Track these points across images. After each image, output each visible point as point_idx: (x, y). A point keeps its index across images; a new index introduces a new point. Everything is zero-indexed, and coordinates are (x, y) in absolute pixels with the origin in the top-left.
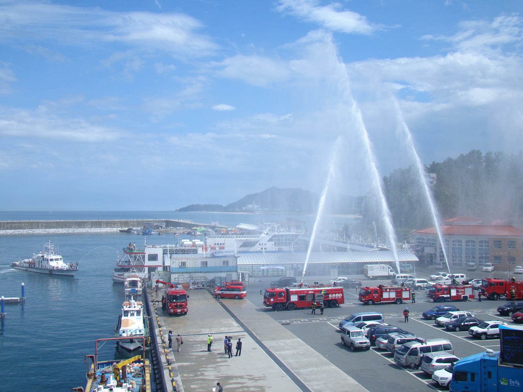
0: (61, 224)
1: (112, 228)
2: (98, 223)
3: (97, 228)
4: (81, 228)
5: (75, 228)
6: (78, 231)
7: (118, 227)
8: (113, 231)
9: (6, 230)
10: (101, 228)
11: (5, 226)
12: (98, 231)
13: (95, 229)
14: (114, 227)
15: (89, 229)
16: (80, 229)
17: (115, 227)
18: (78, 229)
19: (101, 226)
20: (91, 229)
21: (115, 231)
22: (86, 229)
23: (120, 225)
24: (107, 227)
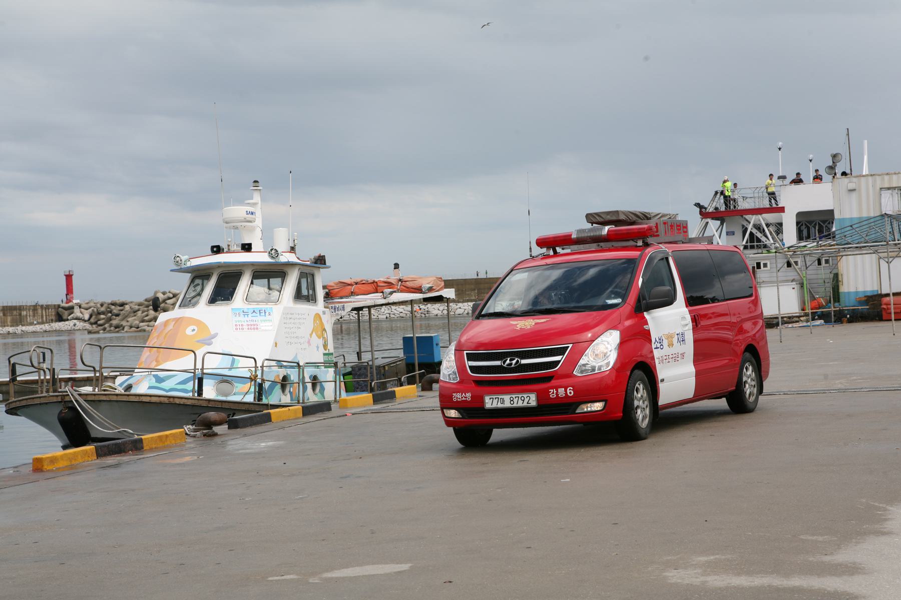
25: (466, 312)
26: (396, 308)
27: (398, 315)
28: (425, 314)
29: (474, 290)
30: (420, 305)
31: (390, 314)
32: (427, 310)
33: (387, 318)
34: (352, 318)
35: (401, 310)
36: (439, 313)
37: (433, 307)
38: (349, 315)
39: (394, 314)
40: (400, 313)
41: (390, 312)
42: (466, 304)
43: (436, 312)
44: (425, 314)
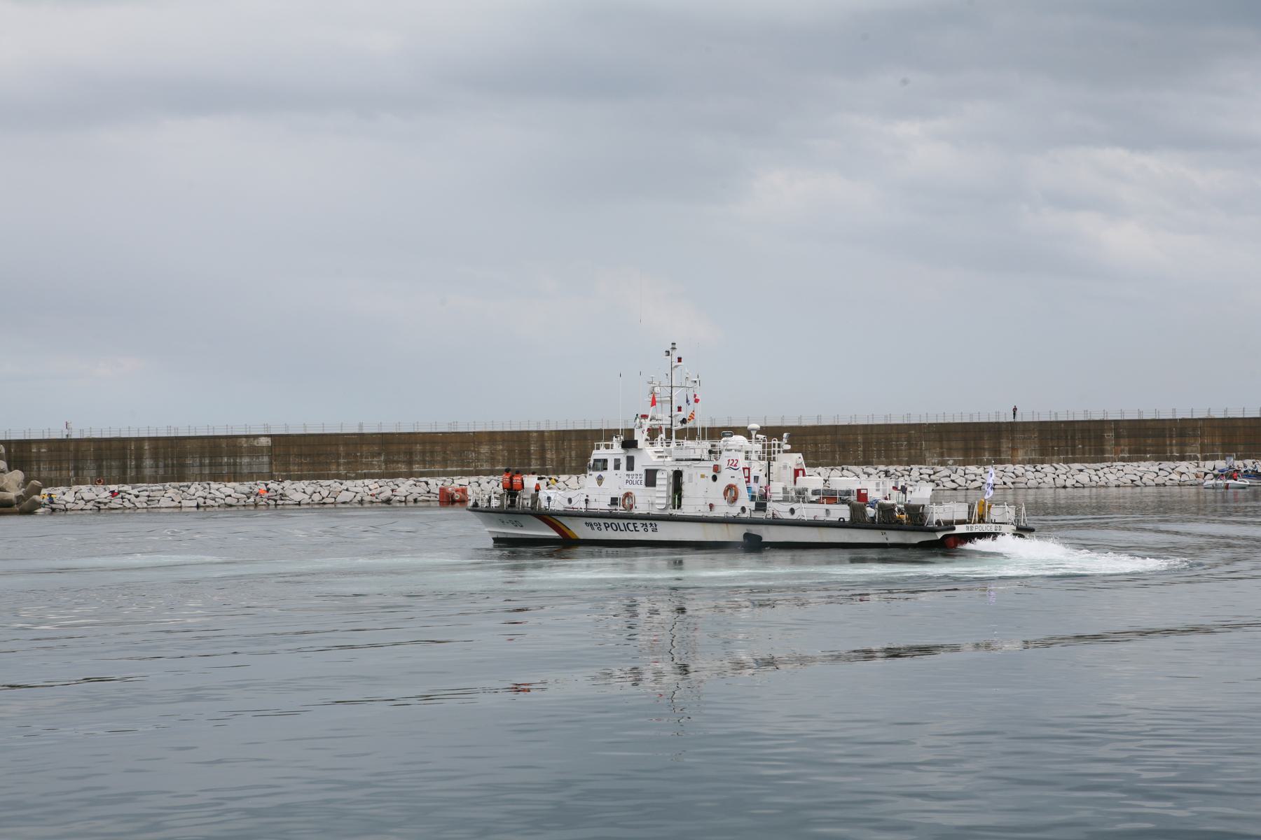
0: (860, 438)
1: (1165, 465)
2: (1078, 435)
3: (1074, 461)
4: (979, 463)
5: (943, 463)
6: (961, 481)
7: (1205, 459)
8: (1175, 477)
9: (557, 472)
10: (1103, 460)
11: (549, 456)
12: (1083, 478)
13: (1062, 468)
14: (1182, 458)
15: (1028, 467)
16: (972, 469)
17: (1190, 459)
18: (961, 469)
19: (1103, 452)
20: (1039, 467)
21: (1189, 478)
22: (1010, 467)
23: (1218, 441)
24: (1137, 454)
25: (358, 498)
26: (222, 486)
27: (223, 502)
28: (276, 501)
29: (380, 454)
30: (269, 482)
31: (205, 498)
32: (281, 491)
33: (198, 506)
34: (127, 504)
35: (229, 491)
36: (306, 498)
37: (294, 486)
38: (122, 498)
39: (214, 499)
40: (226, 497)
41: (205, 495)
42: (359, 482)
43: (298, 497)
44: (276, 501)
